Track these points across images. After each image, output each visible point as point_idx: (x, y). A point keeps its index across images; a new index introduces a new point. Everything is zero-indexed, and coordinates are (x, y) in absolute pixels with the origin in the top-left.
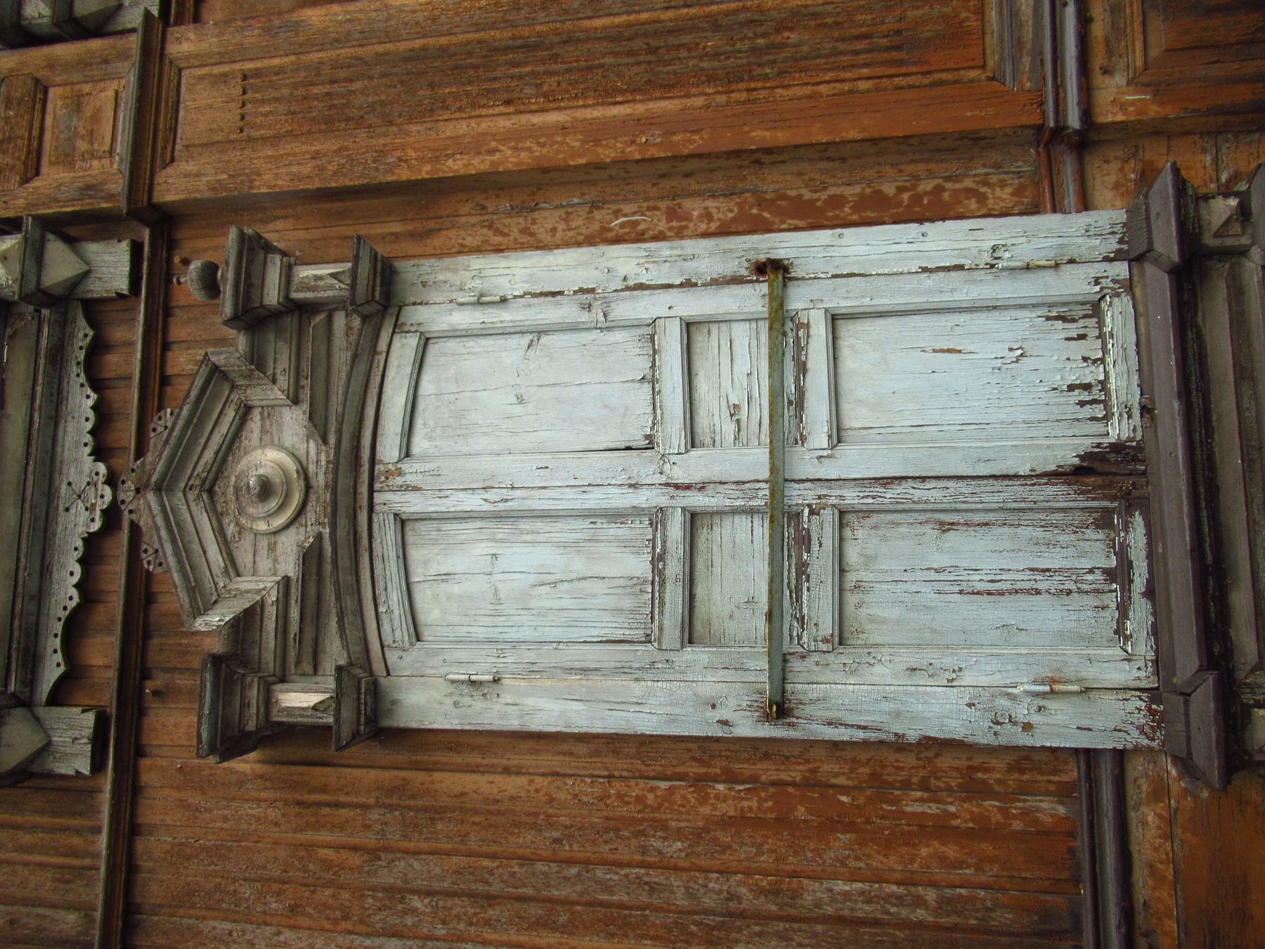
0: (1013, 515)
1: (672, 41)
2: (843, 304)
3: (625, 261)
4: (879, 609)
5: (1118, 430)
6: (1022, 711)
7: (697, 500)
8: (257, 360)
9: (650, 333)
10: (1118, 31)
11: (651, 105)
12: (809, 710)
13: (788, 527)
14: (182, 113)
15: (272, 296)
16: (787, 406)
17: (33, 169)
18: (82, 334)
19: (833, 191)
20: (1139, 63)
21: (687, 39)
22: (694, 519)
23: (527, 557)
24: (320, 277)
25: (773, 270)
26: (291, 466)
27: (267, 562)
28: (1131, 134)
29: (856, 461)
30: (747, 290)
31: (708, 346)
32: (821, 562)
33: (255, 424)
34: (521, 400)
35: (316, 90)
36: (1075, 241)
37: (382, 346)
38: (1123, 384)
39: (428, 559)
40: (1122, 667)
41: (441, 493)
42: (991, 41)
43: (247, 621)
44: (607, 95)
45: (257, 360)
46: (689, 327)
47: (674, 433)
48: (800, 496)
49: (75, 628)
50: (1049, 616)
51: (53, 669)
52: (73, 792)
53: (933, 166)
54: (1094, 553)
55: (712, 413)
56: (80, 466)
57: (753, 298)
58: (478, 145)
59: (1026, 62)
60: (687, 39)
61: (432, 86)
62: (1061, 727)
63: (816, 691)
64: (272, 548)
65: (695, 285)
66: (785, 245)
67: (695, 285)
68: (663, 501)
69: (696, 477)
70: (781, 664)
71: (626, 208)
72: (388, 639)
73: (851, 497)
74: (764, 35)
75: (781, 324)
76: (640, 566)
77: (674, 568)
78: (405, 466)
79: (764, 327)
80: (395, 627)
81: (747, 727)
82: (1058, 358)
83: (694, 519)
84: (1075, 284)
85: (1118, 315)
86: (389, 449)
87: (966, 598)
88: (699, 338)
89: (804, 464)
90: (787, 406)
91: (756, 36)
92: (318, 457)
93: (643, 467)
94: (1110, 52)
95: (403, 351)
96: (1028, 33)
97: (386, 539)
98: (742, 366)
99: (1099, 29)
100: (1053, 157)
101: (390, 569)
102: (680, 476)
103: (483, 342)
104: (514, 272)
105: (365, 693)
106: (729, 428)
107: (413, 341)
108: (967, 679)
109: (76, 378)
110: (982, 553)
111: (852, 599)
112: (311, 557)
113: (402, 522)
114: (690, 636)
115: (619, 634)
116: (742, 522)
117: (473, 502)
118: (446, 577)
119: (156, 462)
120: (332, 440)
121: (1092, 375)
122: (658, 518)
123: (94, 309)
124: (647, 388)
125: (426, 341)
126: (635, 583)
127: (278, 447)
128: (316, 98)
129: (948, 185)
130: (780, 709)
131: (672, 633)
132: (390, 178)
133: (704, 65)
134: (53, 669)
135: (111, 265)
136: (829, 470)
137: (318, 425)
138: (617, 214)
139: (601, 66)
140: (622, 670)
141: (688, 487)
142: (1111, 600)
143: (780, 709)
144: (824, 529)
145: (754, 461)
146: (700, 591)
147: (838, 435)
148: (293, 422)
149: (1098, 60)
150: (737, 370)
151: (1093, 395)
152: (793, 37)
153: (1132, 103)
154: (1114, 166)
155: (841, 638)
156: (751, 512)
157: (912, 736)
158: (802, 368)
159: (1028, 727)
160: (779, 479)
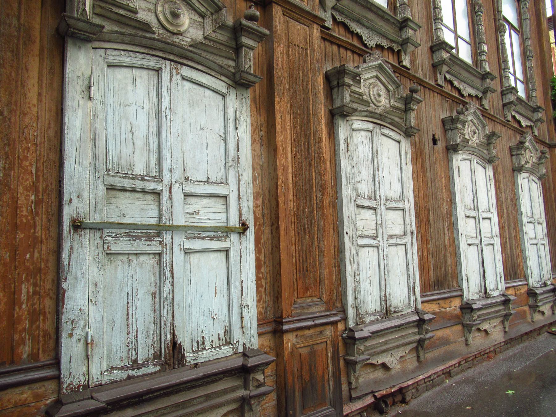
1: (308, 198)
2: (232, 253)
3: (247, 175)
4: (121, 270)
5: (189, 357)
6: (78, 332)
7: (165, 195)
8: (222, 27)
9: (224, 182)
10: (306, 338)
11: (291, 189)
12: (77, 240)
13: (157, 230)
14: (297, 23)
15: (245, 40)
16: (198, 232)
19: (263, 250)
20: (298, 346)
21: (308, 203)
22: (158, 194)
23: (143, 121)
25: (244, 227)
26: (182, 29)
28: (278, 349)
29: (179, 258)
30: (237, 219)
31: (218, 204)
32: (141, 245)
33: (197, 18)
34: (202, 129)
35: (301, 74)
36: (249, 335)
37: (223, 78)
38: (205, 356)
39: (142, 76)
40: (97, 371)
41: (169, 90)
42: (303, 300)
44: (295, 175)
45: (222, 27)
46: (226, 197)
47: (191, 188)
48: (167, 237)
50: (118, 340)
53: (269, 284)
54: (143, 353)
57: (234, 222)
59: (299, 311)
60: (308, 203)
61: (300, 115)
62: (71, 350)
63: (86, 242)
64: (149, 10)
65: (239, 201)
66: (251, 233)
67: (239, 201)
68: (165, 182)
69: (174, 196)
70: (98, 228)
71: (260, 177)
72: (109, 52)
73: (166, 258)
74: (308, 227)
75: (227, 231)
76: (139, 170)
77: (139, 184)
78: (180, 77)
79: (225, 225)
80: (115, 57)
81: (68, 212)
82: (213, 331)
83: (158, 194)
84: (237, 335)
85: (227, 351)
86: (186, 72)
87: (126, 305)
88: (221, 201)
89: (178, 239)
90: (198, 232)
91: (308, 225)
92: (185, 41)
93: (177, 175)
94: (301, 336)
95: (221, 86)
96: (306, 311)
98: (212, 216)
99: (307, 332)
100: (274, 324)
101: (139, 60)
102: (175, 189)
103: (222, 118)
104: (245, 133)
105: (89, 36)
106: (191, 210)
107: (224, 90)
108: (92, 308)
110: (144, 311)
111: (125, 258)
112: (146, 27)
113: (158, 71)
114: (109, 188)
115: (110, 157)
116: (156, 214)
117: (165, 103)
118: (135, 84)
120: (191, 49)
121: (207, 345)
122: (158, 179)
124: (205, 179)
125: (223, 96)
126: (131, 167)
128: (299, 73)
129: (263, 290)
130: (78, 226)
131: (112, 181)
132: (276, 94)
133: (301, 208)
136: (176, 249)
137: (196, 45)
138: (258, 174)
139: (302, 174)
140: (95, 157)
141: (170, 193)
142: (125, 363)
143: (78, 226)
144: (154, 247)
145: (179, 220)
146: (128, 194)
147: (188, 252)
149: (300, 333)
150: (211, 214)
151: (201, 346)
152: (307, 237)
153: (288, 345)
154: (268, 343)
155: (109, 254)
156: (160, 217)
157: (65, 286)
158: (212, 239)
159: (71, 335)
160: (173, 229)
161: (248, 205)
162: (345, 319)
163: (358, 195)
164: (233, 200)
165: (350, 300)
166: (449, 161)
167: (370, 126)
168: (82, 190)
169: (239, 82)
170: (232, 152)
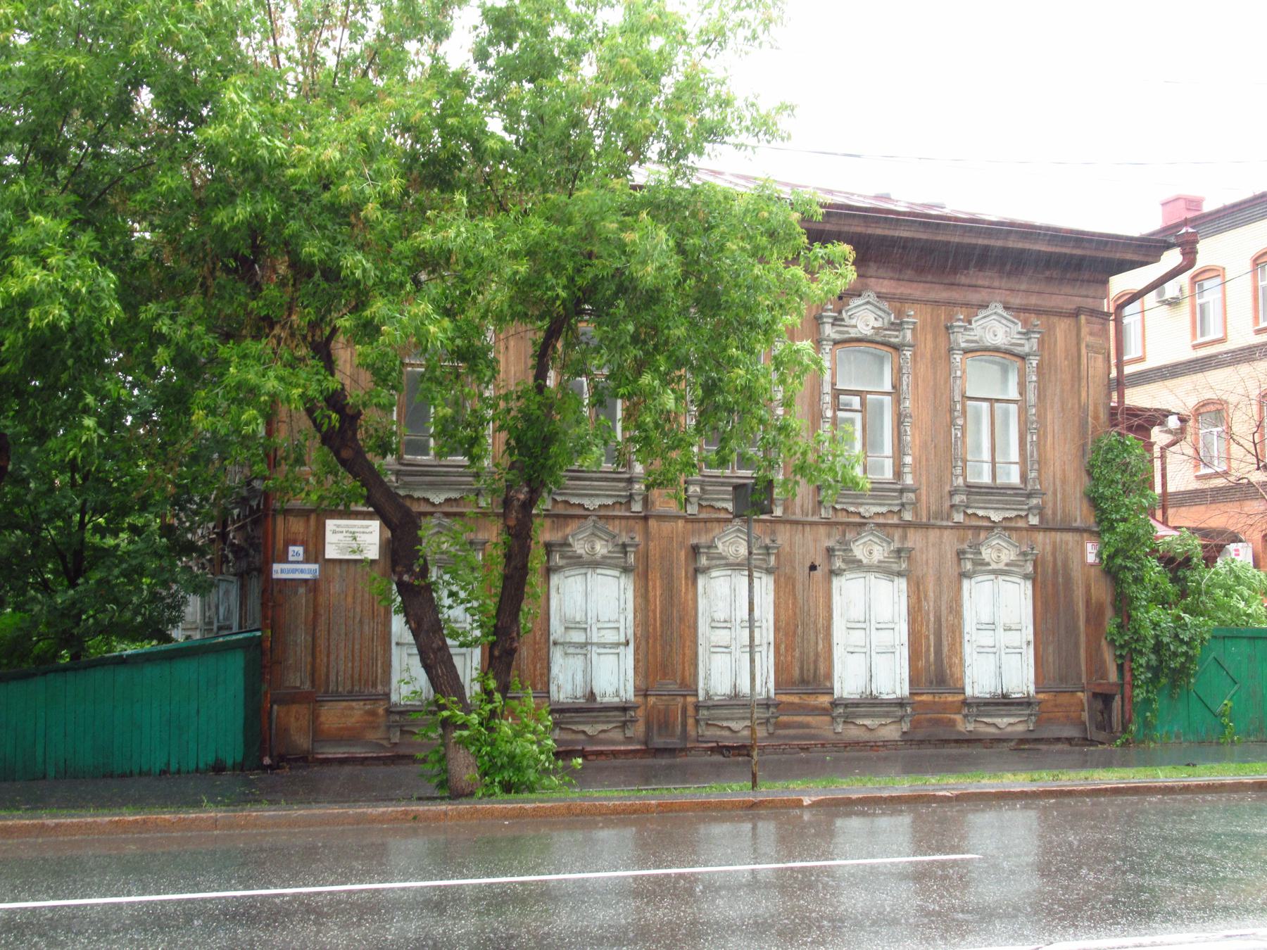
0: (585, 682)
3: (631, 617)
4: (571, 660)
5: (598, 699)
9: (618, 621)
13: (584, 645)
16: (604, 645)
18: (624, 501)
22: (585, 629)
23: (579, 598)
24: (631, 559)
25: (627, 643)
27: (580, 548)
28: (646, 703)
29: (595, 657)
31: (615, 632)
32: (578, 651)
36: (629, 694)
38: (606, 700)
39: (579, 579)
40: (562, 698)
44: (661, 613)
47: (600, 625)
49: (566, 502)
50: (569, 687)
51: (559, 498)
54: (579, 694)
55: (603, 632)
56: (598, 502)
57: (623, 640)
58: (654, 588)
62: (553, 688)
70: (562, 644)
75: (618, 645)
80: (567, 573)
82: (610, 690)
83: (585, 629)
84: (622, 693)
85: (617, 699)
86: (599, 571)
89: (594, 648)
90: (604, 645)
92: (598, 557)
93: (594, 620)
95: (617, 573)
97: (583, 571)
100: (642, 692)
101: (577, 572)
104: (630, 595)
109: (614, 500)
110: (579, 678)
112: (580, 557)
114: (567, 628)
127: (601, 548)
130: (555, 644)
137: (604, 557)
143: (555, 644)
144: (584, 651)
145: (595, 640)
148: (604, 551)
150: (611, 637)
151: (604, 695)
155: (566, 654)
160: (592, 644)
161: (630, 632)
162: (697, 695)
163: (713, 620)
164: (622, 630)
165: (701, 685)
166: (830, 582)
167: (729, 572)
169: (626, 570)
170: (622, 606)
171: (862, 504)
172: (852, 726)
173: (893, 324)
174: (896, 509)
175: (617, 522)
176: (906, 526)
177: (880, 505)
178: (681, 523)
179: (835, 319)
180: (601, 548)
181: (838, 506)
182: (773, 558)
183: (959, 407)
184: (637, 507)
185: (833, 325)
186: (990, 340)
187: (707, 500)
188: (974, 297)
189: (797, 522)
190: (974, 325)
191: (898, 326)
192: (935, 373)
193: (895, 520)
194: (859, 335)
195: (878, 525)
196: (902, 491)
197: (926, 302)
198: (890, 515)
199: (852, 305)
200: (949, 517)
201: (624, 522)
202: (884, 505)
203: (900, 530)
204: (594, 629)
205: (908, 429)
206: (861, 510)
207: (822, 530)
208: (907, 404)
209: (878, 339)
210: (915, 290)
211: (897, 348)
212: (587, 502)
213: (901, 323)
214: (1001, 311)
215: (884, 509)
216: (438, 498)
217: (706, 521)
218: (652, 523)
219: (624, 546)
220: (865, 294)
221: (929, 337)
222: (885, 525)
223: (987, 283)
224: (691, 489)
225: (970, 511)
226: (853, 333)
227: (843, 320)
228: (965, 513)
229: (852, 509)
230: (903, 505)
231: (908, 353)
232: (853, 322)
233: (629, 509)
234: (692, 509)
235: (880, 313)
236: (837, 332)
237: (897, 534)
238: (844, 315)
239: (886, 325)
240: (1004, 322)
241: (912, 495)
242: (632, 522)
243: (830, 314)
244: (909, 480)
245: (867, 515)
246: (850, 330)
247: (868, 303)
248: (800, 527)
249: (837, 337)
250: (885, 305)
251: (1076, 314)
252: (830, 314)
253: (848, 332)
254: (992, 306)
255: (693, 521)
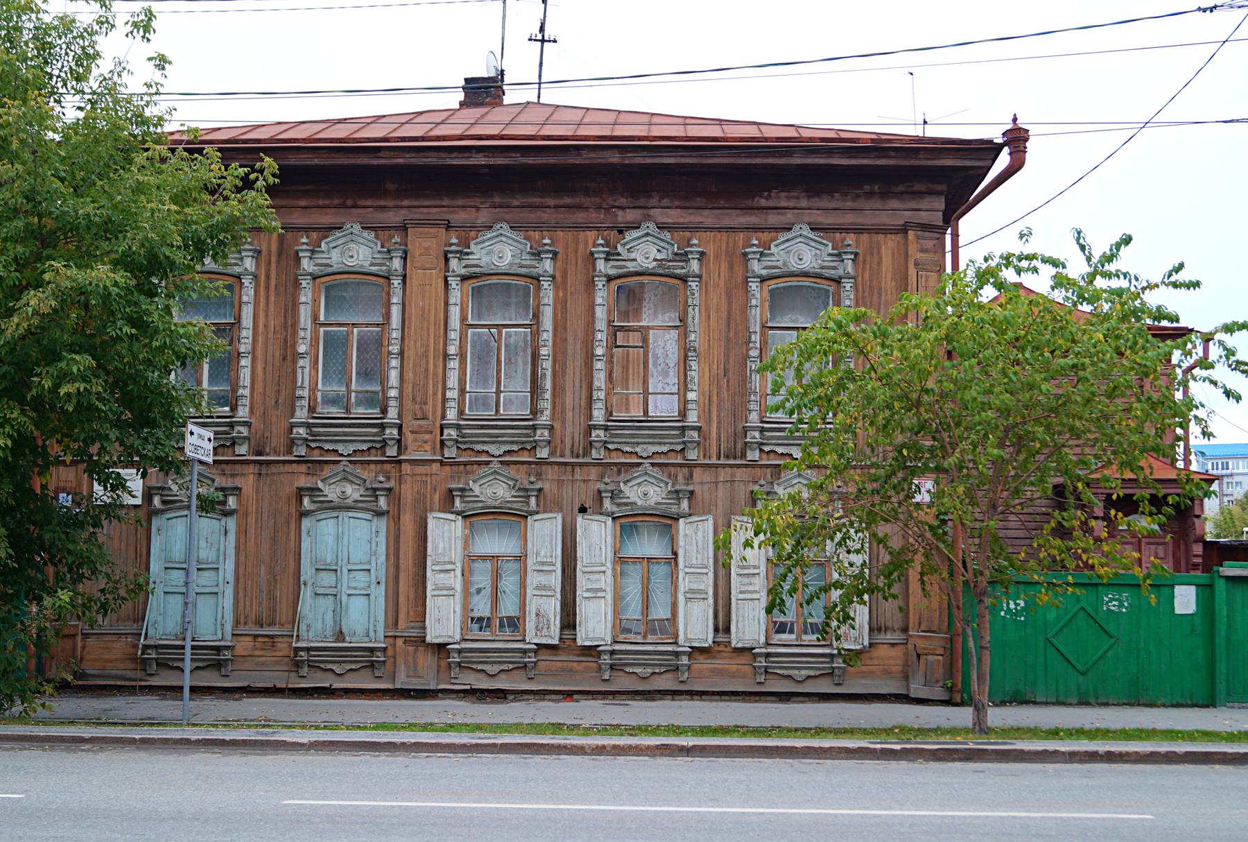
0: (335, 621)
5: (348, 639)
17: (412, 432)
18: (378, 446)
23: (330, 541)
24: (382, 502)
27: (332, 492)
31: (366, 573)
43: (320, 490)
50: (320, 626)
51: (313, 445)
52: (290, 452)
66: (383, 586)
82: (360, 630)
92: (349, 501)
93: (345, 561)
95: (368, 516)
97: (334, 514)
104: (382, 539)
105: (307, 514)
109: (369, 445)
110: (329, 618)
119: (350, 468)
122: (337, 564)
123: (383, 447)
127: (353, 492)
134: (313, 445)
135: (392, 451)
148: (356, 496)
164: (373, 571)
168: (307, 571)
171: (638, 444)
172: (620, 673)
173: (676, 254)
174: (679, 448)
175: (372, 466)
176: (691, 466)
177: (660, 444)
178: (436, 466)
179: (608, 253)
180: (353, 492)
181: (610, 446)
182: (533, 500)
183: (756, 338)
184: (392, 451)
185: (607, 260)
186: (794, 265)
187: (465, 443)
188: (774, 219)
189: (565, 464)
190: (773, 249)
191: (683, 257)
192: (730, 304)
193: (680, 461)
194: (639, 269)
195: (653, 465)
196: (683, 429)
197: (719, 229)
198: (672, 454)
199: (628, 238)
200: (743, 455)
201: (379, 466)
202: (664, 444)
203: (686, 470)
204: (345, 571)
205: (693, 363)
206: (638, 449)
207: (594, 472)
208: (692, 337)
209: (661, 271)
210: (707, 217)
211: (684, 279)
212: (341, 448)
213: (686, 253)
214: (806, 231)
215: (665, 449)
216: (494, 450)
217: (465, 464)
218: (406, 468)
219: (375, 490)
220: (644, 225)
221: (724, 266)
222: (666, 465)
223: (791, 204)
224: (446, 432)
225: (766, 449)
226: (631, 267)
227: (619, 254)
228: (761, 450)
229: (628, 449)
230: (684, 443)
231: (694, 284)
232: (633, 256)
233: (384, 454)
234: (450, 452)
235: (662, 244)
236: (613, 267)
237: (681, 474)
238: (620, 248)
239: (671, 257)
240: (813, 244)
241: (695, 434)
242: (388, 467)
243: (601, 249)
244: (693, 418)
245: (644, 455)
246: (629, 264)
247: (647, 234)
248: (569, 468)
249: (612, 272)
250: (667, 235)
251: (904, 230)
252: (601, 249)
253: (625, 267)
254: (796, 228)
255: (451, 465)
